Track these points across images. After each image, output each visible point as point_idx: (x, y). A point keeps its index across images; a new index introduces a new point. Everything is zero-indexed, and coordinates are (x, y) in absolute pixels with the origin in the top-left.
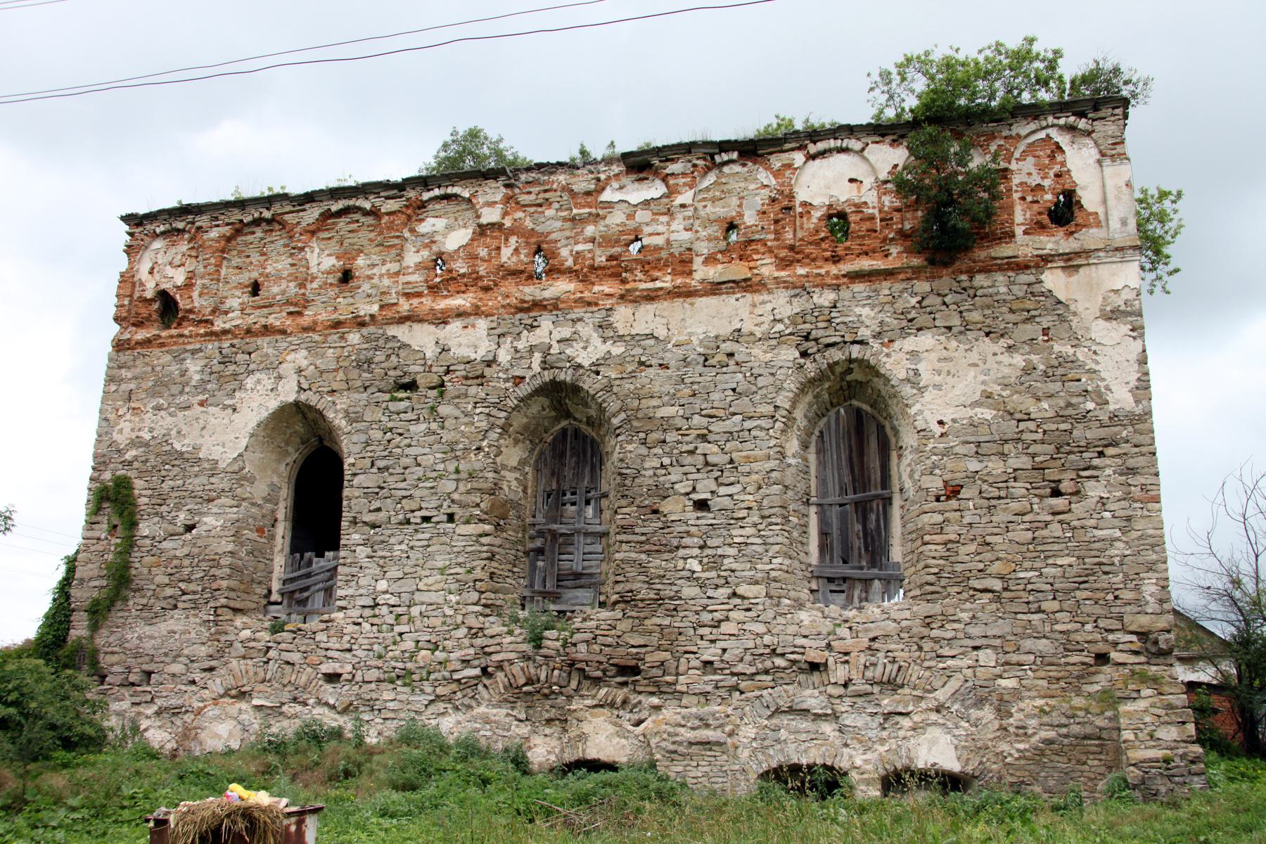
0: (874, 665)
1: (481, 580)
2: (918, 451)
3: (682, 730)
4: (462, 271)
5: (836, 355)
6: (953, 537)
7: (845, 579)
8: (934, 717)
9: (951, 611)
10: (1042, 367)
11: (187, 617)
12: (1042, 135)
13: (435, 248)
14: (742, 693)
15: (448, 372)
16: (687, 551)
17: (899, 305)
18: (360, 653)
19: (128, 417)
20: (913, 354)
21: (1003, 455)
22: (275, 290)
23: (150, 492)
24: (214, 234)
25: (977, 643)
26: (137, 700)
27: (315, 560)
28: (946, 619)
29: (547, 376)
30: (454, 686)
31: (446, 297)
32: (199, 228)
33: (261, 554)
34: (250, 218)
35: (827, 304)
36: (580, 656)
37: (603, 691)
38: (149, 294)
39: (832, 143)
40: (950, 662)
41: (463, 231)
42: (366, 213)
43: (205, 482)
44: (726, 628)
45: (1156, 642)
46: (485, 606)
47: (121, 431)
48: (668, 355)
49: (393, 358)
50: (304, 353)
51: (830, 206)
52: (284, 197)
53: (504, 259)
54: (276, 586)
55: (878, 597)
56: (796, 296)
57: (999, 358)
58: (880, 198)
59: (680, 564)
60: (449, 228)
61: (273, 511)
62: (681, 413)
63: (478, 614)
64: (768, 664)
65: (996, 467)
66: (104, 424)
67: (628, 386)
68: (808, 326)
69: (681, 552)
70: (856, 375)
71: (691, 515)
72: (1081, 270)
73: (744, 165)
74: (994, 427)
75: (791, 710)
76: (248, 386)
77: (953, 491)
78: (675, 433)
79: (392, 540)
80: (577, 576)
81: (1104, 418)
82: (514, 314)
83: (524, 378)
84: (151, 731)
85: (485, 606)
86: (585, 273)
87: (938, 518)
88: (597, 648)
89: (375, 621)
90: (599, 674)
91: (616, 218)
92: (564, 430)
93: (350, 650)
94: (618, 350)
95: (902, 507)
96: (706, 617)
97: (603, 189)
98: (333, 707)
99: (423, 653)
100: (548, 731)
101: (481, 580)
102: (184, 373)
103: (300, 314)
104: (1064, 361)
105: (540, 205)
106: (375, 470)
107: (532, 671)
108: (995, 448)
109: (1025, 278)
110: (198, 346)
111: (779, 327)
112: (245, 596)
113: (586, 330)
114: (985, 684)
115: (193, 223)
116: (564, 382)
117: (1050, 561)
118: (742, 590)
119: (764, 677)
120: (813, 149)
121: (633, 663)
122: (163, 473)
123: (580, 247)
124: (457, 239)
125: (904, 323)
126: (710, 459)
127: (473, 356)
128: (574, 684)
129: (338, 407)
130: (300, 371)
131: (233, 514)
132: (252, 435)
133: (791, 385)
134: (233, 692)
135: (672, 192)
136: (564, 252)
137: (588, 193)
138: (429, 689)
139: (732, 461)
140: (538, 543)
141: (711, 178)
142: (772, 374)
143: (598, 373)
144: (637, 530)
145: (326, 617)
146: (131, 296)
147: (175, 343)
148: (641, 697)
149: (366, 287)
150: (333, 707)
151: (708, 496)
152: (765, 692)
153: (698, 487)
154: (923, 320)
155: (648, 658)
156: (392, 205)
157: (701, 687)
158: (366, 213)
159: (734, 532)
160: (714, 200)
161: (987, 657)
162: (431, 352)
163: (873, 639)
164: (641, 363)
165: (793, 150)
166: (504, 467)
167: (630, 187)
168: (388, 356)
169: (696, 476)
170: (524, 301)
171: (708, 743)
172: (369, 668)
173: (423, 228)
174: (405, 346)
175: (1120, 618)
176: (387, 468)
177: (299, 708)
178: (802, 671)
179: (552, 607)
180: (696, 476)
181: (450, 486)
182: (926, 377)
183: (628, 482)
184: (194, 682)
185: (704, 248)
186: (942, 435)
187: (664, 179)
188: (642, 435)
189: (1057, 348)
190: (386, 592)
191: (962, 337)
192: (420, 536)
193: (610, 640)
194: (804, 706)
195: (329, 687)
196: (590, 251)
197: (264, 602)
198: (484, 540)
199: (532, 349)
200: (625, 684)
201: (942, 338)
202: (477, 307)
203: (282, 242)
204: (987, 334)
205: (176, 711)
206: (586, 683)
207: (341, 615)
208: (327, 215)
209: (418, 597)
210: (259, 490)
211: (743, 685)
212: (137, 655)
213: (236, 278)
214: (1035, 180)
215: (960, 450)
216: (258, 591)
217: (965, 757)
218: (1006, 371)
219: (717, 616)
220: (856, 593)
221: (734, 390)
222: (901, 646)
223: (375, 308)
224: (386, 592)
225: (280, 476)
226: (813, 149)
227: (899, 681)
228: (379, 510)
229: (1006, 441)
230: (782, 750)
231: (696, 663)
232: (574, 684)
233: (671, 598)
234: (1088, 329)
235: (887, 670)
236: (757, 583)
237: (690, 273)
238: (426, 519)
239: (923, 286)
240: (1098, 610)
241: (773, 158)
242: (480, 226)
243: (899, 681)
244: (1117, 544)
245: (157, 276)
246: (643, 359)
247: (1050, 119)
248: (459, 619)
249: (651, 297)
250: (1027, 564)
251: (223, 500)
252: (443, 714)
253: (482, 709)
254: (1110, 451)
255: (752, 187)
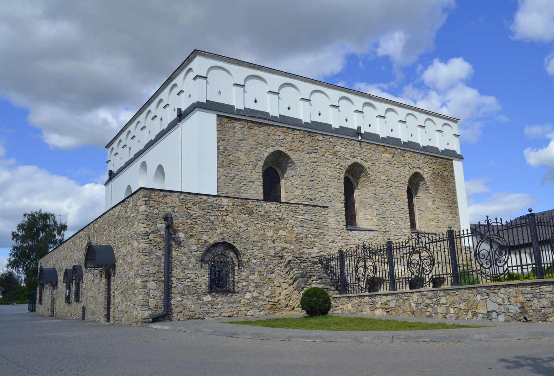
69: (390, 219)
118: (403, 230)
176: (313, 181)
219: (399, 237)
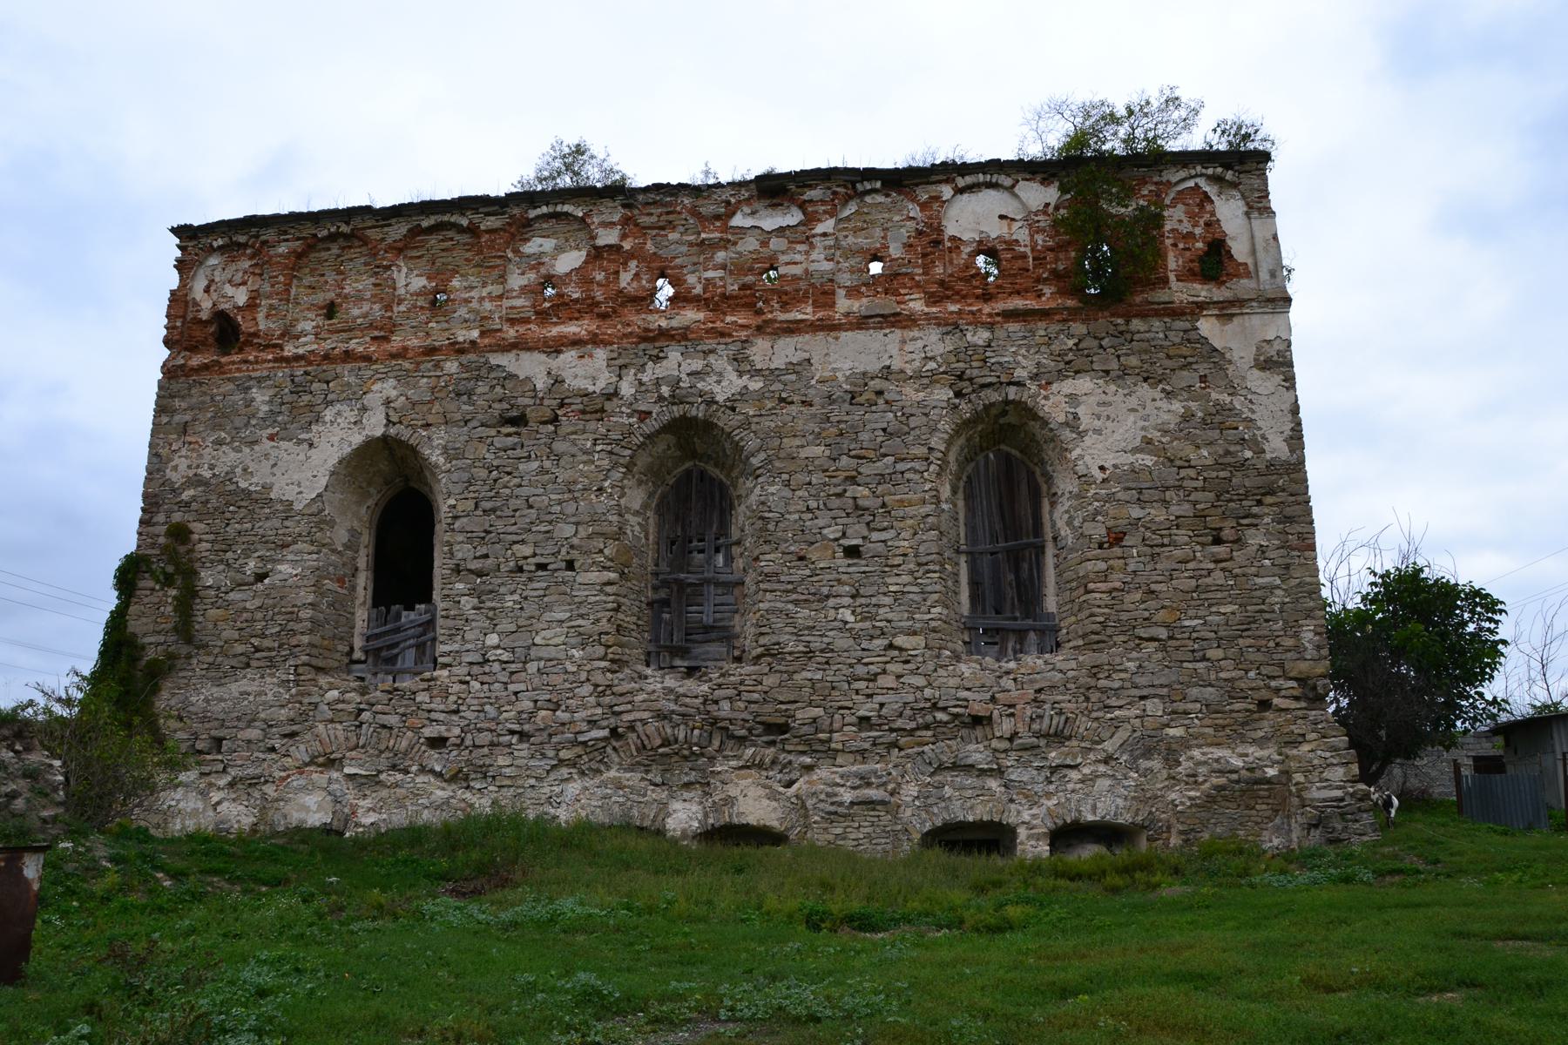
0: (1041, 717)
1: (607, 633)
2: (1079, 496)
3: (842, 790)
4: (575, 296)
5: (994, 396)
6: (1118, 584)
7: (998, 630)
8: (1102, 768)
9: (1118, 660)
10: (1200, 414)
11: (262, 677)
12: (1191, 184)
13: (543, 271)
14: (901, 749)
15: (562, 405)
16: (838, 600)
17: (1056, 347)
18: (468, 714)
19: (184, 452)
20: (1073, 399)
21: (1166, 503)
22: (356, 312)
23: (212, 537)
24: (282, 249)
25: (1145, 692)
26: (207, 769)
27: (404, 613)
28: (1115, 668)
29: (677, 411)
30: (579, 750)
31: (556, 324)
32: (264, 243)
33: (341, 606)
34: (325, 233)
35: (981, 343)
36: (722, 714)
37: (750, 751)
38: (204, 316)
39: (981, 177)
40: (1117, 713)
41: (575, 254)
42: (461, 230)
43: (278, 525)
44: (883, 681)
45: (1314, 688)
46: (612, 661)
47: (175, 468)
48: (812, 392)
49: (498, 389)
50: (392, 382)
51: (980, 242)
52: (367, 210)
53: (623, 284)
54: (358, 643)
55: (1034, 649)
56: (947, 333)
57: (1159, 404)
58: (1032, 236)
59: (832, 612)
60: (559, 250)
61: (354, 559)
62: (827, 453)
63: (604, 670)
64: (929, 718)
65: (1158, 514)
66: (155, 460)
67: (768, 423)
68: (961, 365)
69: (832, 602)
70: (1012, 418)
71: (841, 561)
72: (1236, 320)
73: (887, 196)
74: (1155, 474)
75: (955, 767)
76: (327, 419)
77: (1116, 538)
78: (821, 475)
79: (503, 590)
80: (707, 629)
81: (1261, 466)
82: (637, 344)
83: (650, 413)
84: (226, 804)
85: (612, 661)
86: (715, 302)
87: (1102, 566)
88: (742, 705)
89: (486, 678)
90: (743, 732)
91: (750, 244)
92: (688, 473)
93: (457, 712)
94: (756, 385)
95: (1056, 556)
96: (861, 670)
97: (734, 213)
98: (439, 775)
99: (543, 713)
100: (686, 795)
101: (607, 633)
102: (249, 403)
103: (386, 339)
104: (1221, 409)
105: (662, 228)
106: (479, 512)
107: (669, 731)
108: (1156, 495)
109: (1180, 324)
110: (265, 373)
111: (932, 365)
112: (326, 653)
113: (720, 362)
114: (1153, 733)
115: (257, 237)
116: (696, 418)
117: (1214, 609)
118: (900, 641)
119: (924, 733)
120: (961, 182)
121: (782, 720)
122: (228, 515)
123: (710, 274)
124: (569, 261)
125: (1062, 365)
126: (860, 502)
127: (591, 389)
128: (716, 743)
129: (436, 443)
130: (388, 402)
131: (312, 561)
132: (333, 474)
133: (945, 426)
134: (321, 760)
135: (810, 219)
136: (691, 279)
137: (718, 217)
138: (551, 753)
139: (884, 505)
140: (663, 594)
141: (852, 208)
142: (926, 415)
143: (733, 409)
144: (783, 578)
145: (427, 675)
146: (184, 317)
147: (239, 370)
148: (791, 757)
149: (462, 312)
150: (439, 775)
151: (858, 541)
152: (926, 748)
153: (849, 532)
154: (1079, 363)
155: (799, 715)
156: (492, 222)
157: (855, 745)
158: (461, 230)
159: (889, 580)
160: (856, 231)
161: (1154, 707)
162: (541, 383)
163: (1039, 691)
164: (782, 400)
165: (940, 182)
166: (628, 509)
167: (763, 212)
168: (493, 387)
169: (845, 521)
170: (647, 330)
171: (872, 802)
172: (480, 730)
173: (531, 247)
174: (512, 376)
175: (1281, 665)
176: (494, 510)
177: (399, 776)
178: (965, 725)
179: (678, 662)
180: (845, 521)
181: (568, 530)
182: (1086, 422)
183: (771, 527)
184: (273, 749)
185: (846, 279)
186: (1104, 481)
187: (802, 206)
188: (784, 477)
189: (1214, 395)
190: (498, 647)
191: (1120, 382)
192: (536, 585)
193: (756, 696)
194: (969, 761)
195: (434, 754)
196: (721, 279)
197: (346, 660)
198: (609, 589)
199: (658, 382)
200: (772, 743)
201: (1101, 382)
202: (596, 335)
203: (362, 260)
204: (1145, 380)
205: (254, 782)
206: (730, 743)
207: (445, 673)
208: (416, 231)
209: (534, 652)
210: (341, 536)
211: (902, 741)
212: (204, 719)
213: (305, 299)
214: (1186, 227)
215: (1121, 496)
216: (340, 648)
217: (1134, 808)
218: (1166, 417)
220: (1010, 645)
221: (884, 430)
222: (1068, 697)
223: (475, 334)
224: (498, 647)
225: (360, 520)
226: (961, 182)
227: (1067, 732)
228: (486, 556)
229: (1168, 488)
230: (947, 808)
231: (853, 719)
232: (716, 743)
233: (822, 651)
234: (1244, 378)
235: (1054, 722)
236: (915, 633)
237: (832, 305)
238: (542, 567)
239: (1079, 328)
240: (1260, 657)
241: (919, 190)
242: (596, 248)
243: (1067, 732)
244: (1279, 592)
245: (214, 296)
246: (784, 395)
247: (1199, 168)
248: (583, 676)
249: (792, 329)
250: (1191, 613)
251: (300, 546)
252: (567, 780)
253: (613, 773)
254: (1269, 500)
255: (897, 218)
